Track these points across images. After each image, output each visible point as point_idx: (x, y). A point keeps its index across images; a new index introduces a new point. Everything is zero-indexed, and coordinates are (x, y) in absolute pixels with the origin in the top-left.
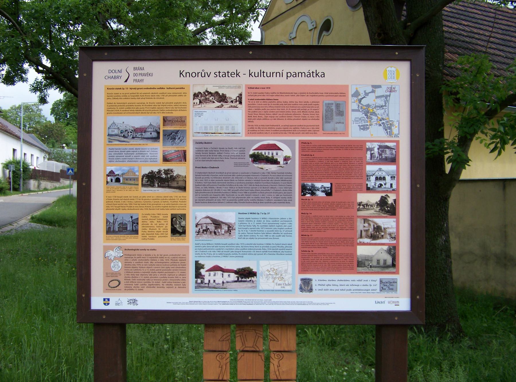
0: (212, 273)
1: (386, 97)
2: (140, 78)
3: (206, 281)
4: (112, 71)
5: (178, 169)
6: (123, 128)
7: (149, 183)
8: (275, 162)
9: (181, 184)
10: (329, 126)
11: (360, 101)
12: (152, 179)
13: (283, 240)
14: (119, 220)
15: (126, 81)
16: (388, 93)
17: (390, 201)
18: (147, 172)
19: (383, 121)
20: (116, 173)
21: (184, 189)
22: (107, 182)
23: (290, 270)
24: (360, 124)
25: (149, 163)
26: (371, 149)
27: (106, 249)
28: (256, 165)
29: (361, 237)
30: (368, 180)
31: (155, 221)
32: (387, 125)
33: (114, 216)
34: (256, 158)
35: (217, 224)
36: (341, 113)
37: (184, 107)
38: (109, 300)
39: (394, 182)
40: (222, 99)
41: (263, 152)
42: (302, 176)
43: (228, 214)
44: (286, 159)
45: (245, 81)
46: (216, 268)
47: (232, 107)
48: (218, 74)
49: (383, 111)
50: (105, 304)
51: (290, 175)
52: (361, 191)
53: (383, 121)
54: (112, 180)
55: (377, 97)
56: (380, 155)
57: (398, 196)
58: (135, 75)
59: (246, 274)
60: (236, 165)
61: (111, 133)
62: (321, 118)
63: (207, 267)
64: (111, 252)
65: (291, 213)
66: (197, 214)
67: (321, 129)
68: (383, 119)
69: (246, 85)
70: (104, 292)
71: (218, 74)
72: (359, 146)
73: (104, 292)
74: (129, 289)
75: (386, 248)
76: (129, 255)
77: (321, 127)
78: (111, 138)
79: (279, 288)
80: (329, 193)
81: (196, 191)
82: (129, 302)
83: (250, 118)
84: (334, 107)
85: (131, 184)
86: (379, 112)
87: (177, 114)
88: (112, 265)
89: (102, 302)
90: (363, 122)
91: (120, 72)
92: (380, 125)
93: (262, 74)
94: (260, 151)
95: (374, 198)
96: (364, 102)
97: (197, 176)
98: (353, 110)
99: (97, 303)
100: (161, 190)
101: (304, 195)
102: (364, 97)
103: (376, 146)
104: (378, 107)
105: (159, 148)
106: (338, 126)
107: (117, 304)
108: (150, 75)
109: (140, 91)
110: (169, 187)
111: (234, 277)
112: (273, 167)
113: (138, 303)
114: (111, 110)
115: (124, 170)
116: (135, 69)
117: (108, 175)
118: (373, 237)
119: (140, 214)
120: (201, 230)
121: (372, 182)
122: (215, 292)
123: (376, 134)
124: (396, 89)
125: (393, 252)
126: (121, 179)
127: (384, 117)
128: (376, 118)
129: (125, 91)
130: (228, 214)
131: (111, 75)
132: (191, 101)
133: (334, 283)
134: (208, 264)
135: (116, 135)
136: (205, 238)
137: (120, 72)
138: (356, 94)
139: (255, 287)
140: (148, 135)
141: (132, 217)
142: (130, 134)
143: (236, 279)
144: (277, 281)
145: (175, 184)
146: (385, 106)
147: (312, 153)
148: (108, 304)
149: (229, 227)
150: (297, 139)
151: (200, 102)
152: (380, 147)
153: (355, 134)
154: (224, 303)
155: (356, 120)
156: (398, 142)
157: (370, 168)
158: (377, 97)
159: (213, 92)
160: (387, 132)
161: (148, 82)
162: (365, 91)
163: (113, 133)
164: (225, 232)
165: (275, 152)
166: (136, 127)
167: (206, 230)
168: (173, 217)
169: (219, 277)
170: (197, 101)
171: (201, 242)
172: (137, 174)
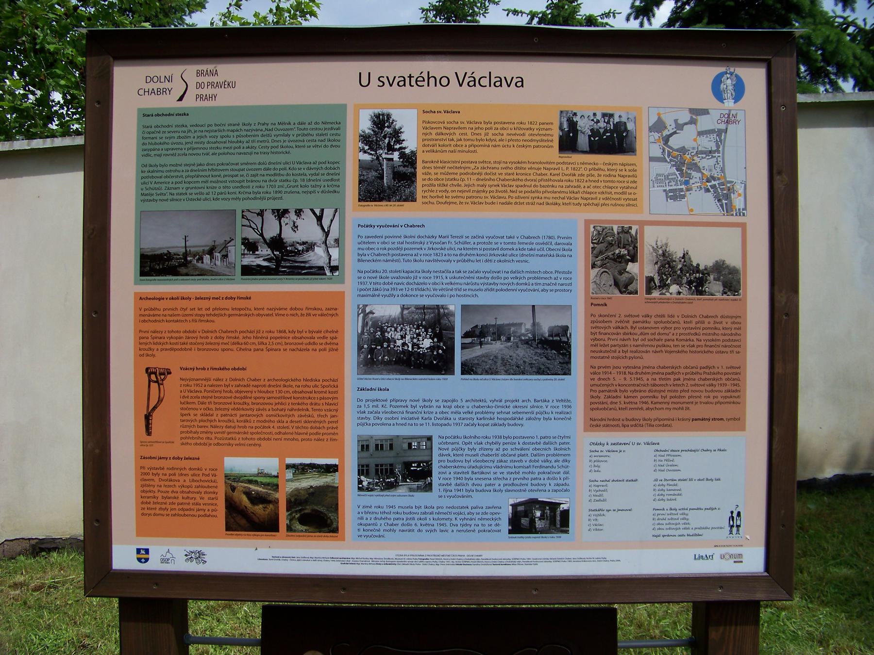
1: (719, 133)
4: (152, 79)
11: (666, 140)
15: (181, 99)
16: (723, 126)
19: (713, 183)
24: (668, 188)
32: (722, 190)
38: (147, 551)
49: (712, 162)
50: (139, 560)
53: (713, 183)
55: (700, 134)
58: (199, 85)
68: (714, 179)
82: (189, 557)
86: (705, 163)
89: (135, 555)
90: (673, 183)
91: (169, 79)
92: (707, 190)
96: (674, 142)
98: (652, 159)
99: (123, 558)
102: (675, 133)
104: (702, 152)
107: (165, 561)
108: (230, 85)
113: (206, 558)
124: (738, 118)
128: (699, 175)
131: (151, 86)
137: (169, 79)
138: (658, 126)
146: (718, 151)
148: (147, 560)
155: (659, 180)
158: (700, 134)
160: (722, 206)
161: (225, 98)
162: (676, 121)
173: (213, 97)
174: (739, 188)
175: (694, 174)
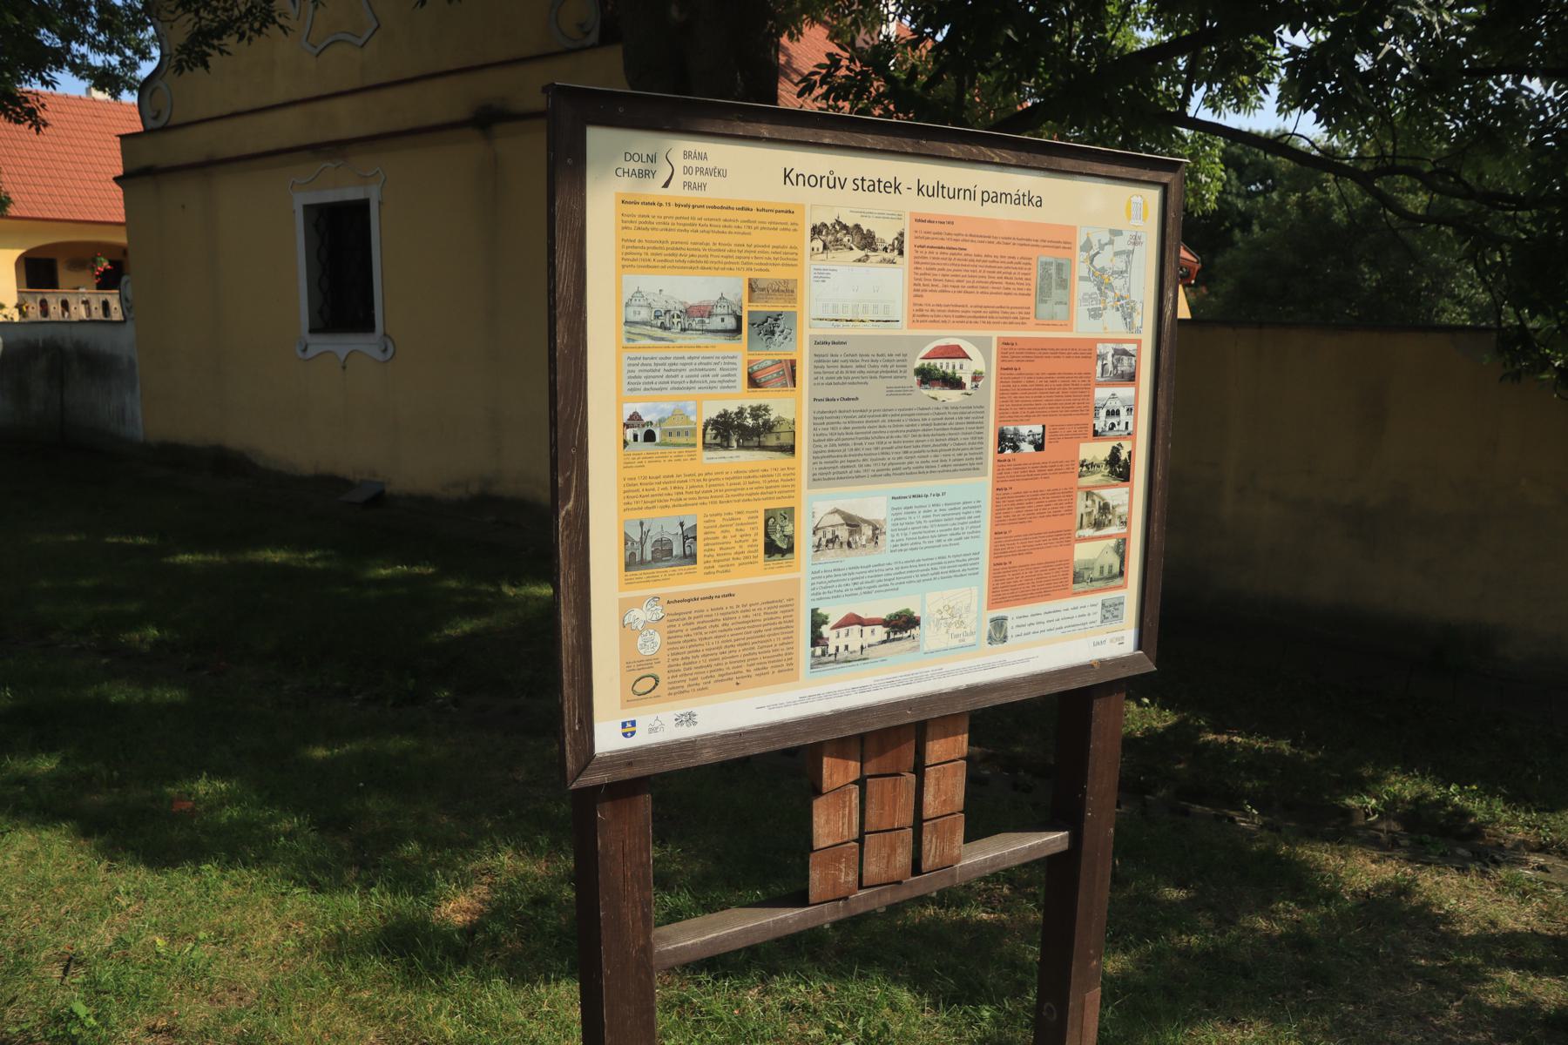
0: (843, 631)
1: (1129, 253)
2: (696, 178)
3: (831, 650)
5: (779, 404)
6: (660, 305)
7: (718, 440)
8: (954, 383)
9: (785, 439)
10: (1044, 309)
12: (727, 431)
13: (966, 546)
14: (654, 535)
15: (666, 185)
17: (1124, 455)
18: (714, 416)
20: (646, 419)
21: (790, 449)
22: (626, 443)
23: (974, 607)
25: (719, 391)
26: (1102, 357)
27: (626, 606)
28: (925, 392)
29: (1081, 527)
30: (1096, 416)
31: (732, 530)
33: (642, 524)
34: (927, 377)
35: (853, 524)
36: (1064, 284)
37: (790, 257)
38: (633, 723)
39: (1130, 419)
40: (868, 241)
41: (938, 362)
42: (1002, 414)
43: (871, 502)
44: (976, 377)
45: (911, 203)
46: (851, 620)
47: (884, 261)
48: (860, 184)
50: (625, 735)
51: (981, 409)
52: (1085, 439)
54: (635, 438)
55: (1116, 254)
56: (1115, 367)
57: (1134, 445)
58: (687, 170)
59: (902, 624)
60: (891, 392)
61: (632, 318)
62: (1033, 292)
63: (833, 621)
64: (637, 613)
65: (978, 489)
66: (816, 506)
67: (1032, 315)
69: (912, 214)
70: (623, 708)
71: (860, 184)
72: (1086, 350)
73: (623, 708)
74: (677, 692)
75: (1112, 542)
76: (677, 614)
77: (1032, 311)
78: (633, 330)
79: (955, 643)
80: (1039, 447)
81: (816, 455)
82: (679, 721)
83: (917, 289)
84: (1053, 271)
85: (679, 445)
86: (1118, 283)
87: (777, 273)
88: (640, 641)
89: (620, 731)
93: (939, 190)
94: (932, 362)
95: (1098, 451)
96: (1098, 262)
97: (817, 419)
98: (1082, 279)
100: (745, 455)
101: (1002, 451)
103: (1108, 349)
105: (739, 353)
106: (1058, 308)
107: (652, 730)
108: (720, 173)
109: (697, 212)
110: (762, 447)
111: (881, 632)
112: (952, 396)
113: (697, 719)
114: (630, 258)
115: (663, 411)
116: (687, 155)
117: (627, 426)
118: (1098, 525)
119: (694, 515)
120: (824, 542)
121: (1101, 422)
122: (847, 669)
123: (1111, 326)
125: (1121, 550)
126: (657, 433)
127: (1124, 293)
129: (664, 211)
130: (871, 502)
132: (808, 244)
133: (1039, 618)
134: (835, 612)
135: (645, 323)
136: (836, 559)
138: (1087, 246)
139: (916, 648)
140: (715, 323)
141: (682, 525)
142: (676, 320)
143: (885, 637)
144: (953, 630)
145: (771, 441)
147: (1017, 365)
148: (633, 733)
149: (875, 529)
150: (995, 334)
151: (825, 247)
152: (1116, 352)
153: (1083, 327)
154: (863, 689)
156: (1139, 342)
157: (1101, 394)
158: (1116, 254)
159: (850, 224)
161: (716, 190)
163: (638, 318)
164: (869, 541)
165: (957, 362)
166: (690, 303)
167: (832, 541)
168: (769, 516)
169: (854, 638)
170: (818, 244)
171: (821, 568)
172: (693, 418)
173: (702, 186)
174: (1139, 306)
175: (1110, 294)
